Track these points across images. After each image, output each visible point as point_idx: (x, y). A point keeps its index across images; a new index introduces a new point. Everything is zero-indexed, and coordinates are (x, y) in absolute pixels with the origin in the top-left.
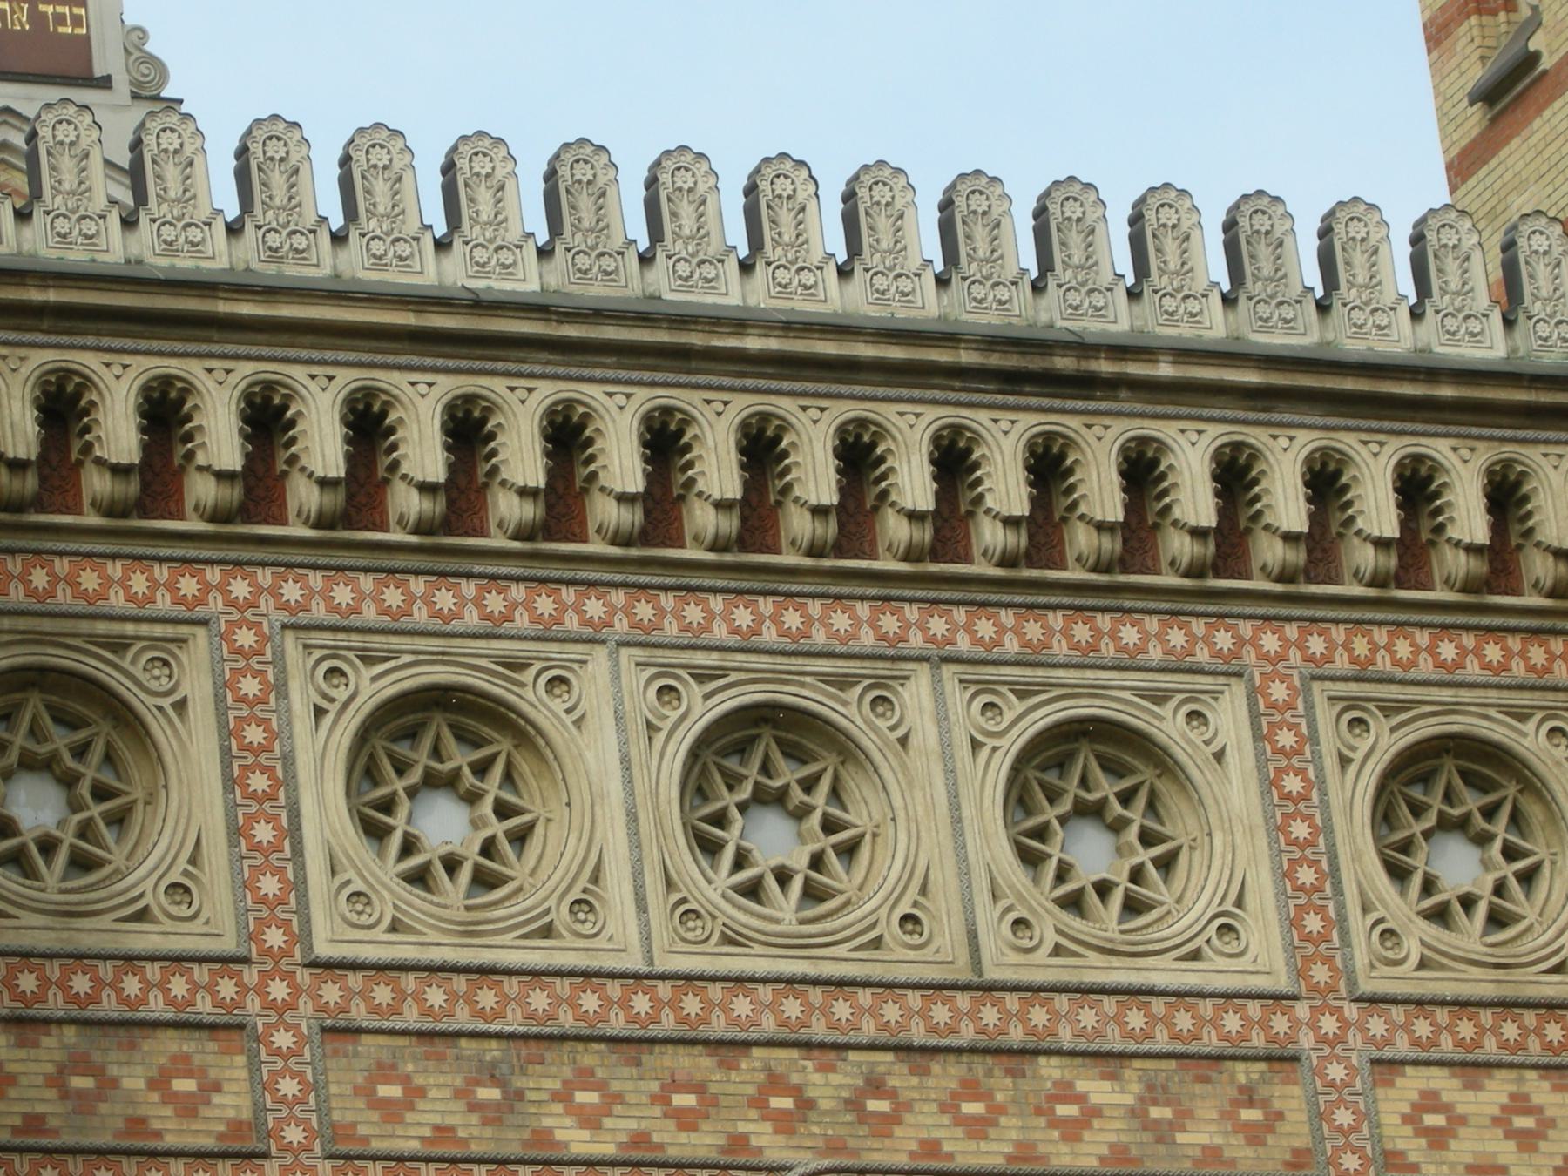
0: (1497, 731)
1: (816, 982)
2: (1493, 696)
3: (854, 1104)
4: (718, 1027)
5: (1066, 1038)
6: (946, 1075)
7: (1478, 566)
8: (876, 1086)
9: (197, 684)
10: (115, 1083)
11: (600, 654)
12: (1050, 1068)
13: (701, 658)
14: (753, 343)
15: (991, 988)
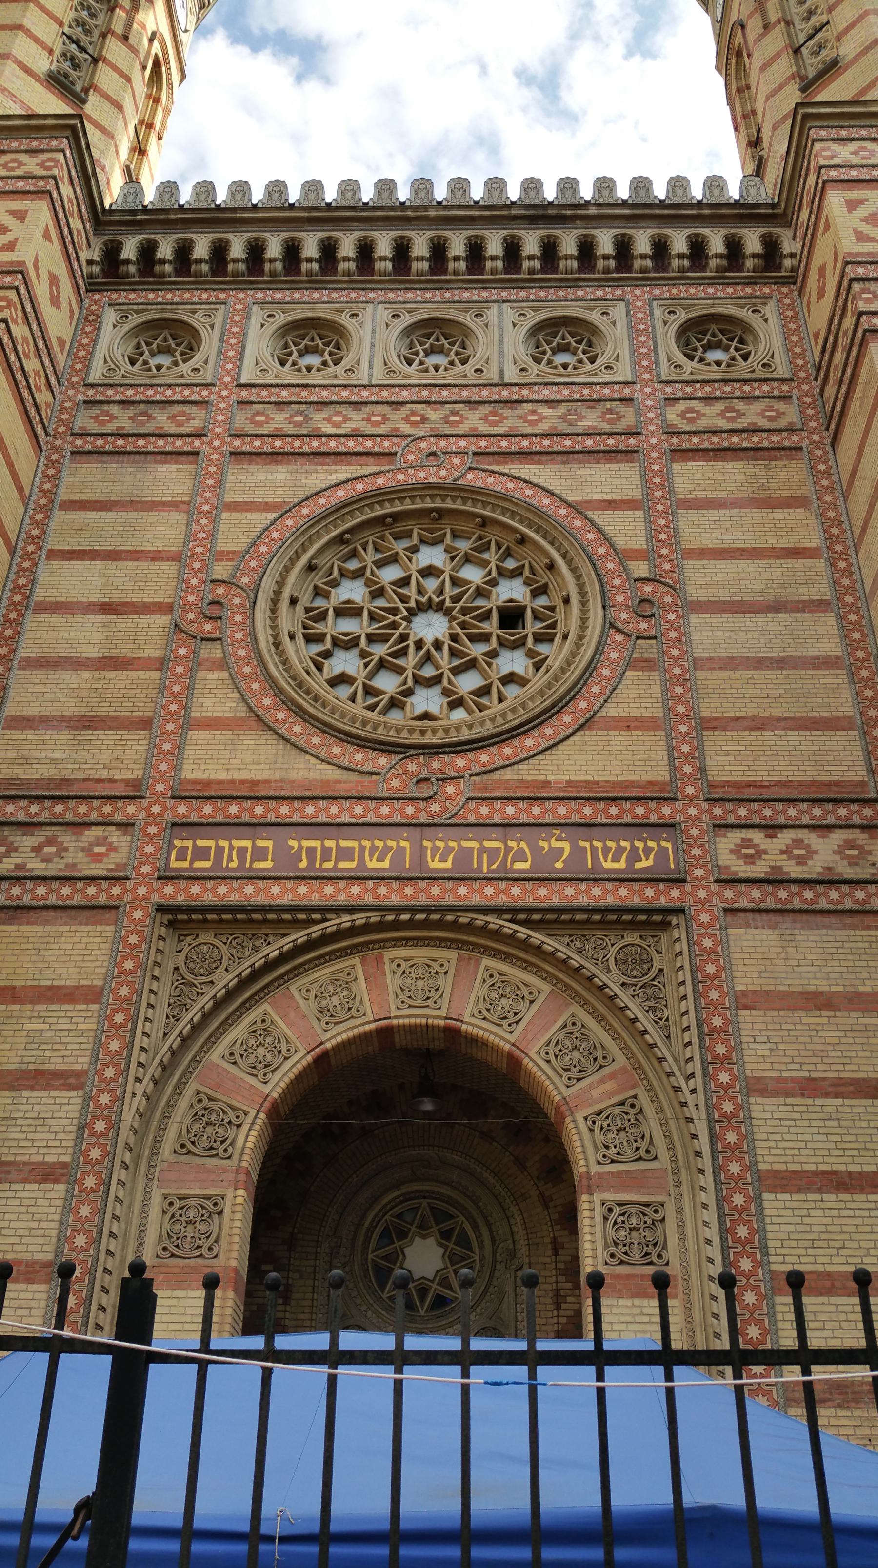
0: (732, 311)
1: (435, 385)
2: (729, 301)
3: (445, 419)
4: (394, 398)
5: (535, 397)
6: (484, 410)
7: (725, 262)
8: (455, 414)
9: (218, 321)
10: (155, 418)
11: (371, 305)
12: (528, 407)
13: (409, 305)
14: (432, 213)
15: (506, 385)
